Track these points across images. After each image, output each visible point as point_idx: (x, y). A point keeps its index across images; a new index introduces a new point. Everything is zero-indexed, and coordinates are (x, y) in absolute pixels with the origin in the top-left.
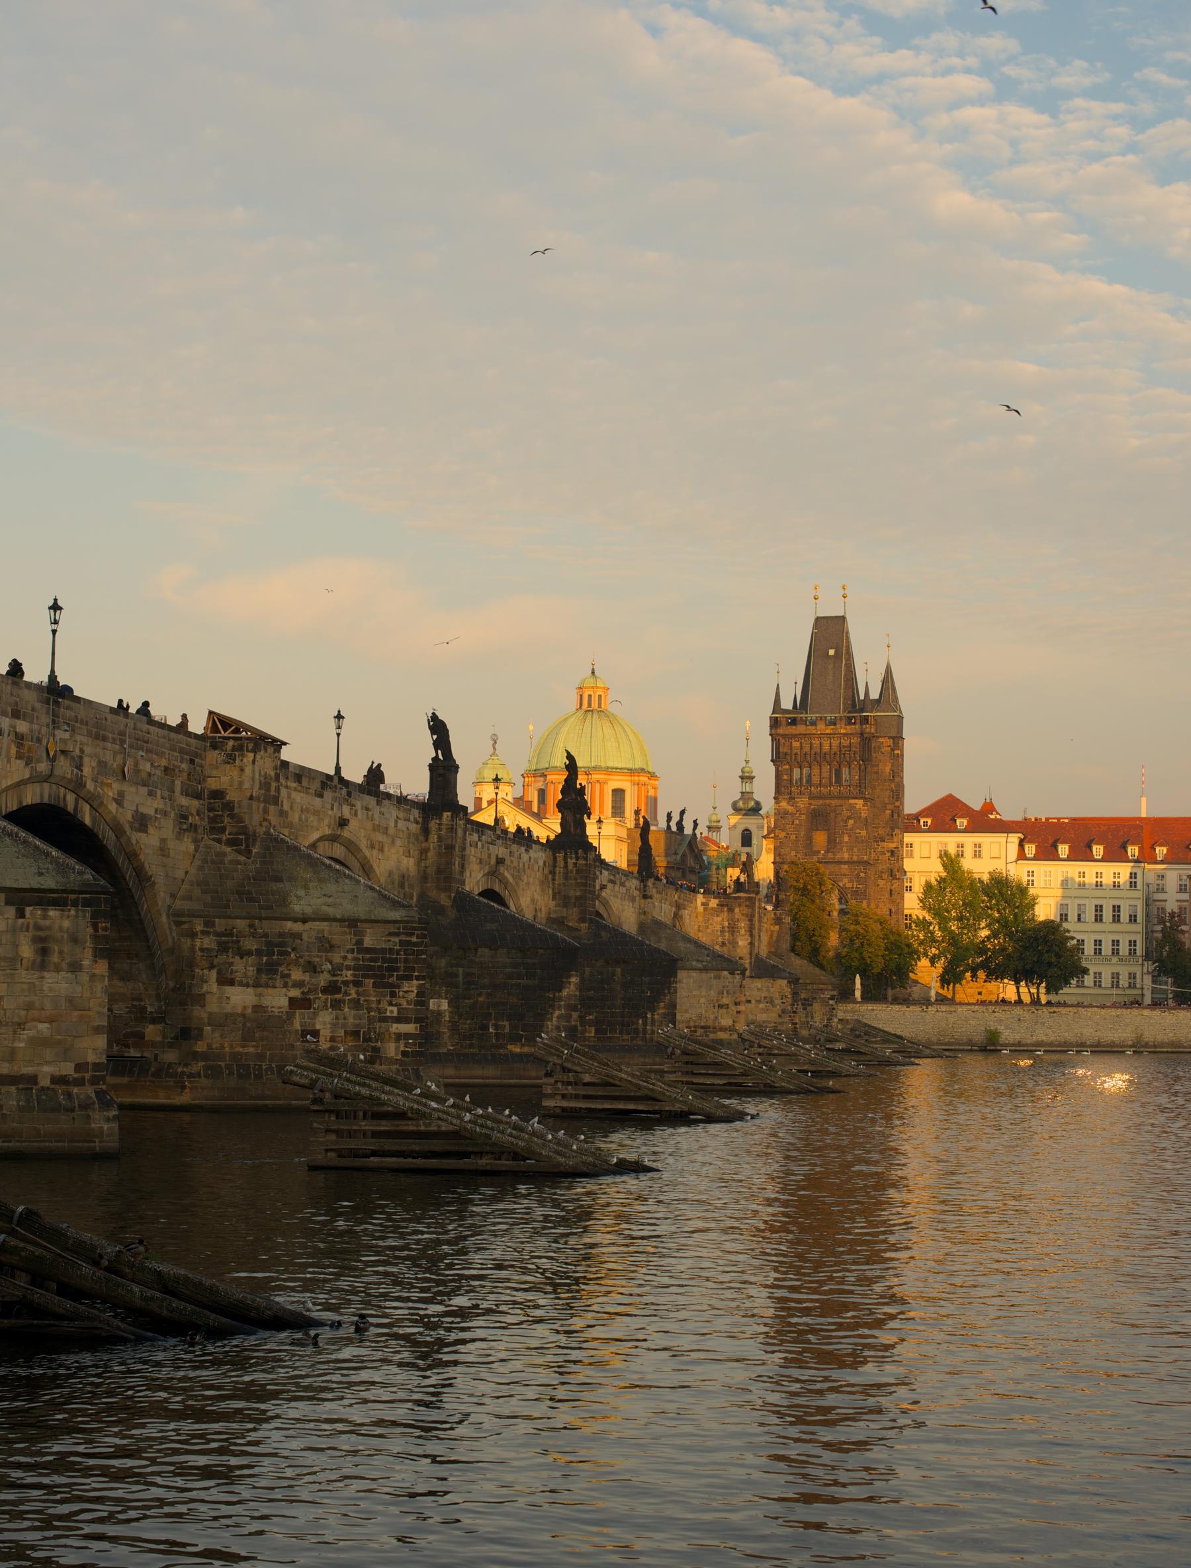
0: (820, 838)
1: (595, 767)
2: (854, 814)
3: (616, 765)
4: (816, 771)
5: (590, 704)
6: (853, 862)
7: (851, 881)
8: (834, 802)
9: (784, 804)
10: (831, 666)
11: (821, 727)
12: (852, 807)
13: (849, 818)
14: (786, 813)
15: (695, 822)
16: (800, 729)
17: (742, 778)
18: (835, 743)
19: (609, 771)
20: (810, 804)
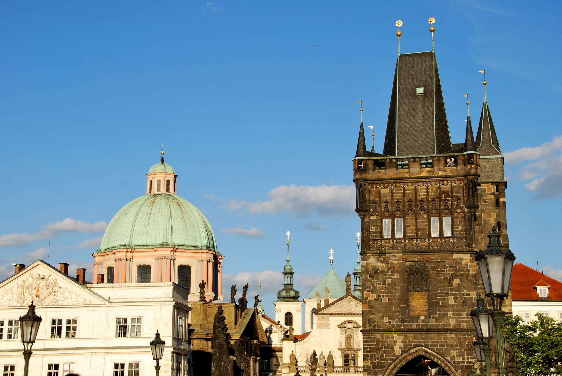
0: (419, 301)
1: (163, 244)
2: (459, 271)
3: (182, 243)
4: (411, 221)
5: (159, 189)
6: (463, 330)
7: (460, 354)
8: (434, 257)
9: (373, 261)
10: (420, 106)
11: (415, 170)
12: (458, 263)
13: (454, 276)
14: (376, 271)
15: (256, 297)
16: (391, 173)
17: (284, 273)
18: (433, 188)
19: (175, 249)
20: (406, 260)
